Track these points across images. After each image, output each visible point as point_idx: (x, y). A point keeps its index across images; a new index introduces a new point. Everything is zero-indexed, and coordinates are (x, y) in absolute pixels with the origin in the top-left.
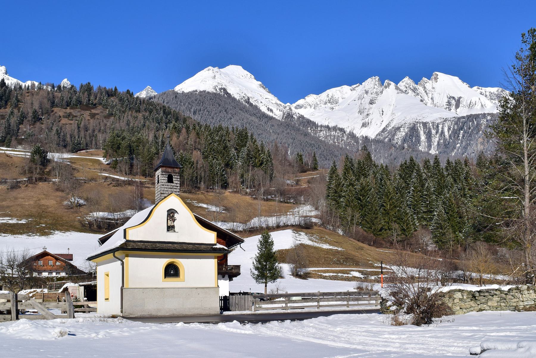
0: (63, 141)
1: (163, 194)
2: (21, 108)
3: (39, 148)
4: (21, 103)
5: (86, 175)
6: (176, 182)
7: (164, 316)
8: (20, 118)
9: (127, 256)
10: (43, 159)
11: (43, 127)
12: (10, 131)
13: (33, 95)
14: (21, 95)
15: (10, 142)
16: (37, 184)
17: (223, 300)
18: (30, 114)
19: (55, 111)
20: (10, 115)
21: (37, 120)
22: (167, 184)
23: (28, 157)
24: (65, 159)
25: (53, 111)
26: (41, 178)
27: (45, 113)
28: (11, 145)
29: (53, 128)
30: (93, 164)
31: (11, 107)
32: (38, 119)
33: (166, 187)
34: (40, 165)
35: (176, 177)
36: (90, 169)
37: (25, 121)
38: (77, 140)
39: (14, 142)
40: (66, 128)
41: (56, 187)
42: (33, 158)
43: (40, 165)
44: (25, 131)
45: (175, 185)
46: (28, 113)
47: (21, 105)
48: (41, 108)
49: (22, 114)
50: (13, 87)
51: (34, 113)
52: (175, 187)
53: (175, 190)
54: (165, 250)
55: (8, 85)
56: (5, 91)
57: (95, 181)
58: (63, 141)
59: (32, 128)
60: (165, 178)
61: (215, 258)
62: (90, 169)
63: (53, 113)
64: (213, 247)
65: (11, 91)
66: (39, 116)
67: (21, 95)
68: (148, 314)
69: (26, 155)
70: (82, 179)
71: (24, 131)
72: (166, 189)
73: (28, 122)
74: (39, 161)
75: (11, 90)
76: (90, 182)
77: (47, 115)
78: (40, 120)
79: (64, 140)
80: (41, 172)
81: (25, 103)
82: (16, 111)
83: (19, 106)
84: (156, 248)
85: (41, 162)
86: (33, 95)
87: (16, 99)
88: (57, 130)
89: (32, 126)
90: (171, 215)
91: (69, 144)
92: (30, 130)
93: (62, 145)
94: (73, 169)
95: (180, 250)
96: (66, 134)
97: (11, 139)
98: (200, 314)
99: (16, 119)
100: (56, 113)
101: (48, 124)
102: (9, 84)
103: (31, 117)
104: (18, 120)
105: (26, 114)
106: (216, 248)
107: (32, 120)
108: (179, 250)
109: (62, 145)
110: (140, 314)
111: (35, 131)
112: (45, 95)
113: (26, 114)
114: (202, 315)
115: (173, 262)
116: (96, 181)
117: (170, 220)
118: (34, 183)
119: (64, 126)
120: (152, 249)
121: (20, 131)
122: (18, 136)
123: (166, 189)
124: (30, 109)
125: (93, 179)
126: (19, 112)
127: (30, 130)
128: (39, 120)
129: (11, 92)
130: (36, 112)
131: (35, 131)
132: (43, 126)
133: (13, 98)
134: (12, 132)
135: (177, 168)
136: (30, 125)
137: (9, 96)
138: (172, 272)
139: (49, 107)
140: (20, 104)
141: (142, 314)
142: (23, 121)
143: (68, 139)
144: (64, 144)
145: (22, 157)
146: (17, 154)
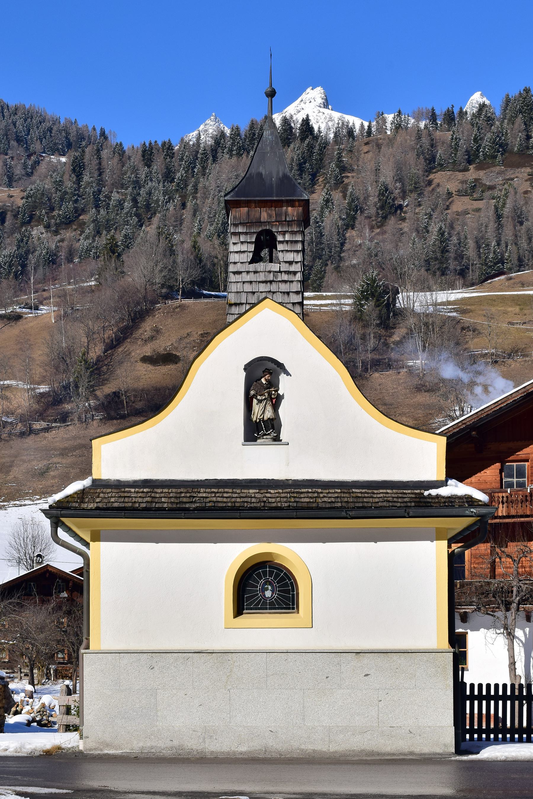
0: (455, 259)
1: (236, 304)
2: (350, 187)
3: (374, 281)
4: (349, 175)
5: (496, 343)
6: (290, 257)
7: (228, 753)
8: (347, 213)
9: (97, 537)
10: (385, 310)
11: (406, 229)
12: (323, 249)
13: (379, 146)
14: (351, 151)
15: (322, 278)
16: (366, 378)
17: (509, 698)
18: (373, 199)
19: (436, 181)
20: (322, 208)
21: (390, 213)
22: (252, 267)
23: (347, 308)
24: (443, 304)
25: (430, 183)
26: (379, 361)
27: (411, 191)
28: (324, 284)
29: (430, 229)
30: (521, 309)
31: (325, 187)
32: (393, 210)
33: (248, 278)
34: (378, 325)
35: (287, 237)
36: (512, 324)
37: (360, 218)
38: (494, 252)
39: (330, 277)
40: (464, 224)
41: (416, 381)
42: (359, 311)
43: (378, 325)
44: (360, 245)
45: (285, 267)
46: (366, 198)
47: (351, 179)
48: (400, 180)
49: (353, 201)
50: (332, 136)
51: (381, 194)
52: (285, 277)
53: (284, 287)
54: (222, 509)
55: (320, 132)
56: (311, 147)
57: (524, 356)
58: (455, 259)
59: (378, 234)
60: (244, 248)
61: (438, 538)
62: (512, 324)
63: (430, 189)
64: (426, 493)
65: (326, 143)
66: (394, 200)
67: (351, 151)
68: (169, 744)
69: (341, 304)
70: (486, 354)
71: (356, 247)
72: (248, 288)
73: (367, 221)
74: (374, 315)
75: (326, 143)
76: (510, 361)
77: (414, 195)
78: (399, 212)
79: (460, 257)
80: (380, 346)
81: (359, 172)
82: (337, 196)
83: (346, 181)
84: (187, 506)
85: (380, 317)
86: (379, 146)
87: (337, 166)
88: (441, 233)
89: (378, 230)
90: (263, 380)
91: (472, 265)
92: (371, 240)
93: (456, 270)
94: (463, 329)
95: (281, 509)
96: (466, 238)
97: (325, 270)
98: (372, 753)
99: (337, 216)
100: (438, 185)
101: (418, 219)
102: (322, 129)
103: (375, 206)
104: (343, 219)
105: (362, 198)
106: (438, 496)
107: (378, 214)
108: (276, 508)
109: (456, 270)
110: (141, 744)
111: (384, 241)
112: (411, 141)
113: (362, 198)
114: (379, 754)
115: (270, 554)
116: (527, 356)
117: (260, 401)
118: (360, 376)
119: (460, 218)
120: (171, 510)
121: (347, 246)
122: (341, 259)
123: (248, 288)
124: (372, 185)
125: (517, 351)
126: (345, 199)
127: (371, 240)
128: (396, 211)
129: (325, 148)
130: (387, 190)
131: (384, 241)
132: (406, 226)
133: (330, 163)
134: (327, 250)
135: (291, 203)
136: (372, 228)
137: (321, 160)
138: (268, 594)
139: (421, 172)
140: (348, 177)
141: (149, 744)
142: (354, 218)
143: (471, 252)
144: (458, 268)
145: (333, 311)
146: (321, 305)
